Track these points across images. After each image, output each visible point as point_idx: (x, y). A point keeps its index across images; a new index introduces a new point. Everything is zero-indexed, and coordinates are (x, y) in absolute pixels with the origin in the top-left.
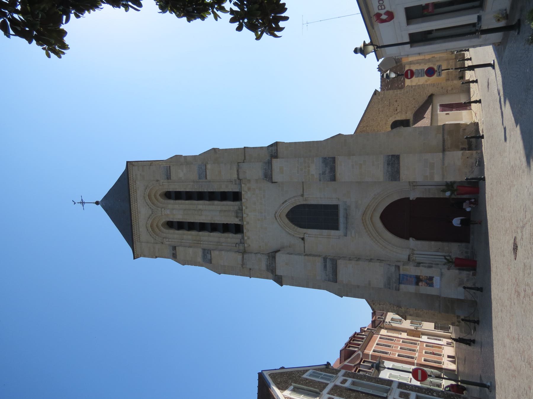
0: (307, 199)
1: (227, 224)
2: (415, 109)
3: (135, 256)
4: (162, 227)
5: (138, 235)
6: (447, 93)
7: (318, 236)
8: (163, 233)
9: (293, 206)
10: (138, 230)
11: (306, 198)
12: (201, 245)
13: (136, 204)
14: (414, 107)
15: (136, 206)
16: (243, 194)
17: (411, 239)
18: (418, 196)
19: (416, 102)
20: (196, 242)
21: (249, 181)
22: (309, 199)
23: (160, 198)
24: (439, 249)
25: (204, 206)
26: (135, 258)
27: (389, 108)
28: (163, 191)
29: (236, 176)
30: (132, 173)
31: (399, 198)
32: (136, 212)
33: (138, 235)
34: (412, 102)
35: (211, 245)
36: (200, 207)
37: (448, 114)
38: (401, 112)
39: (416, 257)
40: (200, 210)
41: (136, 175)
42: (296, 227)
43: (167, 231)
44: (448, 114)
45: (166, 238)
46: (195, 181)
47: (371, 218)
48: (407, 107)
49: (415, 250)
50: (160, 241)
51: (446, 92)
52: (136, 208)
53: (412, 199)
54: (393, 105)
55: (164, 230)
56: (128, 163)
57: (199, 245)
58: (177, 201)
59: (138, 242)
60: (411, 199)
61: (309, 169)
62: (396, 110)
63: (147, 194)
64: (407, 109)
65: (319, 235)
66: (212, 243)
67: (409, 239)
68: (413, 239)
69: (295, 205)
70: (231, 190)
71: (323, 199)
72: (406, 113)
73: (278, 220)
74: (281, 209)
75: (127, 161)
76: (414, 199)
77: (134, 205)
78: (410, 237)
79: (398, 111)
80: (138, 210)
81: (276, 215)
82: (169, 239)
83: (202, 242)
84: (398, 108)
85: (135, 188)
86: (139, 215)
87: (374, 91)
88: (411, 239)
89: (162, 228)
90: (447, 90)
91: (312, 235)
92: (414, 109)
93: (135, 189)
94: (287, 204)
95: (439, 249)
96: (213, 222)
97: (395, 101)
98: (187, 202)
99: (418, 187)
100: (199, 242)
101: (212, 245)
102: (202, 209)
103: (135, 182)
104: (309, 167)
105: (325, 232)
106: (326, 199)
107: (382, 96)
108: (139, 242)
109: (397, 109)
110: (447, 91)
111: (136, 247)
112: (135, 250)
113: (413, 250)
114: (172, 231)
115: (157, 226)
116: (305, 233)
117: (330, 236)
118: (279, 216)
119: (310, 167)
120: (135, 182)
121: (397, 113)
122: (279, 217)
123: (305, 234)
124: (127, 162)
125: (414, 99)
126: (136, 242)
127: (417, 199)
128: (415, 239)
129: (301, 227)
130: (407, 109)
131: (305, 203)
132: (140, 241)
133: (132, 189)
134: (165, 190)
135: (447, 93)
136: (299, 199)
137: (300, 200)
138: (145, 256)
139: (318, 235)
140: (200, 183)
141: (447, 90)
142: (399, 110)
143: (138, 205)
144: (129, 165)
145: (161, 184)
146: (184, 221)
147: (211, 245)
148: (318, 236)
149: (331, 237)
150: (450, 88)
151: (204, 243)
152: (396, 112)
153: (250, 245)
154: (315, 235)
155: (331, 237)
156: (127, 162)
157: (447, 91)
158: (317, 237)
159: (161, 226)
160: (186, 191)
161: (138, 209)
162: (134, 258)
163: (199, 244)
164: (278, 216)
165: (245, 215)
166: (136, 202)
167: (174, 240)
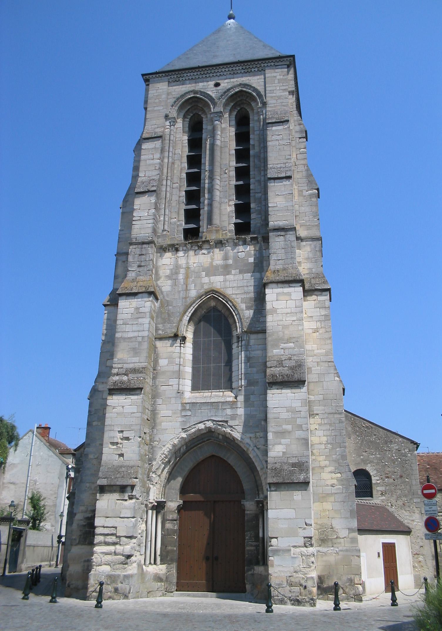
3: (147, 77)
26: (144, 77)
30: (276, 65)
37: (379, 556)
44: (379, 556)
56: (292, 58)
75: (294, 55)
124: (293, 56)
126: (169, 77)
156: (293, 56)
162: (143, 75)
166: (230, 74)
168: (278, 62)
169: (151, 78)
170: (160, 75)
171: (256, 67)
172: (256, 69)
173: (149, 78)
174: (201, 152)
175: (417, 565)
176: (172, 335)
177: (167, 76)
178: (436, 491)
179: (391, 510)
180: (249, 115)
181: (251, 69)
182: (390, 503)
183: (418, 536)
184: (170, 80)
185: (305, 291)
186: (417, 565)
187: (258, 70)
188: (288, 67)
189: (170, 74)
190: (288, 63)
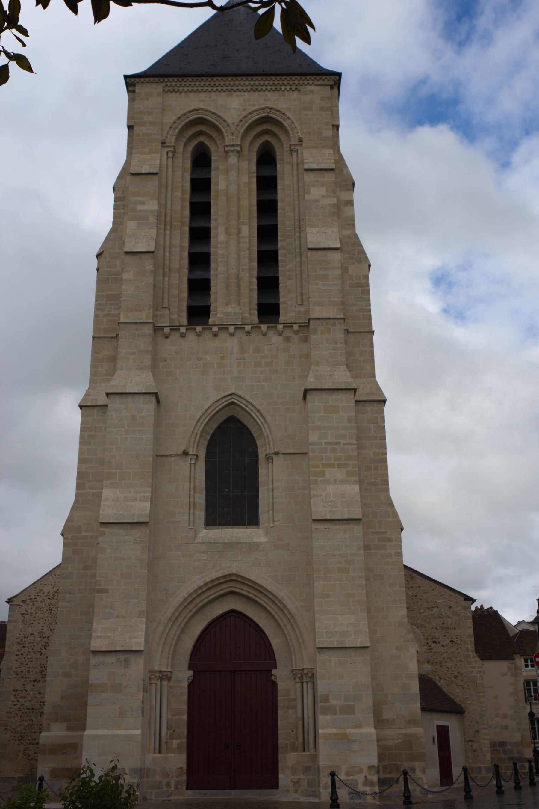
0: (270, 460)
1: (209, 289)
2: (435, 679)
3: (132, 80)
4: (196, 142)
5: (180, 89)
6: (468, 741)
7: (192, 484)
8: (185, 145)
9: (252, 431)
10: (190, 90)
11: (272, 458)
12: (163, 231)
13: (247, 88)
14: (440, 678)
15: (245, 88)
16: (276, 327)
17: (191, 673)
18: (281, 686)
19: (449, 681)
20: (168, 219)
21: (306, 340)
22: (270, 464)
23: (261, 142)
24: (174, 731)
25: (247, 240)
26: (128, 80)
27: (438, 627)
28: (277, 150)
29: (316, 315)
30: (315, 84)
31: (275, 648)
32: (230, 88)
33: (180, 89)
34: (451, 672)
35: (164, 252)
36: (245, 230)
37: (434, 742)
38: (431, 652)
39: (156, 684)
40: (239, 231)
41: (311, 92)
42: (209, 437)
43: (189, 155)
44: (434, 742)
45: (174, 152)
46: (302, 223)
47: (232, 593)
48: (440, 663)
49: (168, 683)
50: (167, 137)
51: (468, 739)
52: (240, 88)
53: (273, 674)
54: (445, 636)
55: (190, 148)
56: (337, 78)
57: (163, 226)
58: (255, 180)
59: (164, 87)
60: (274, 672)
61: (336, 467)
62: (434, 642)
63: (270, 115)
64: (436, 663)
65: (194, 486)
66: (167, 254)
67: (191, 670)
68: (192, 678)
69: (255, 435)
70: (281, 300)
71: (271, 494)
72: (428, 662)
73: (224, 400)
74: (247, 406)
76: (273, 677)
77: (247, 83)
78: (194, 672)
79: (433, 645)
80: (235, 91)
81: (234, 397)
82: (173, 158)
83: (168, 232)
84: (438, 644)
85: (283, 88)
86: (223, 94)
87: (472, 597)
88: (191, 673)
89: (194, 143)
90: (473, 741)
91: (195, 472)
92: (437, 677)
93: (281, 89)
94: (259, 419)
95: (174, 731)
96: (212, 257)
97: (453, 640)
98: (255, 202)
99: (299, 685)
100: (168, 227)
101: (164, 256)
102: (240, 235)
103: (296, 89)
104: (340, 466)
105: (200, 499)
106: (271, 501)
107: (462, 614)
108: (164, 90)
109: (436, 643)
110: (470, 741)
111: (152, 83)
112: (145, 79)
113: (169, 679)
114: (188, 165)
115: (200, 133)
116: (197, 456)
117: (194, 510)
118: (233, 403)
119: (340, 468)
120: (296, 89)
121: (428, 644)
122: (230, 401)
123: (196, 457)
124: (339, 75)
125: (456, 677)
126: (164, 85)
127: (275, 684)
128: (190, 681)
129: (208, 446)
130: (436, 663)
131: (261, 456)
132: (166, 92)
133: (281, 82)
134: (278, 154)
135: (468, 741)
136: (269, 444)
137: (268, 446)
138: (131, 101)
139: (195, 483)
140: (297, 234)
141: (473, 741)
142: (434, 648)
143: (246, 94)
144: (333, 77)
145: (292, 147)
146: (213, 193)
147: (164, 252)
148: (192, 484)
149: (192, 510)
150: (475, 746)
151: (168, 237)
152: (430, 643)
153: (167, 337)
154: (195, 478)
155: (192, 510)
156: (339, 75)
157: (470, 741)
158: (190, 482)
159: (199, 141)
160: (278, 201)
161: (238, 93)
162: (126, 77)
163: (165, 226)
164: (233, 400)
165: (234, 330)
167: (170, 170)
168: (318, 80)
169: (138, 83)
170: (152, 79)
171: (288, 84)
172: (288, 88)
173: (135, 82)
174: (210, 199)
175: (470, 755)
176: (180, 452)
177: (162, 82)
178: (535, 660)
179: (439, 684)
180: (275, 153)
181: (281, 85)
182: (438, 675)
183: (473, 718)
184: (166, 89)
185: (356, 402)
186: (470, 755)
187: (291, 89)
188: (332, 87)
189: (166, 79)
190: (332, 83)
